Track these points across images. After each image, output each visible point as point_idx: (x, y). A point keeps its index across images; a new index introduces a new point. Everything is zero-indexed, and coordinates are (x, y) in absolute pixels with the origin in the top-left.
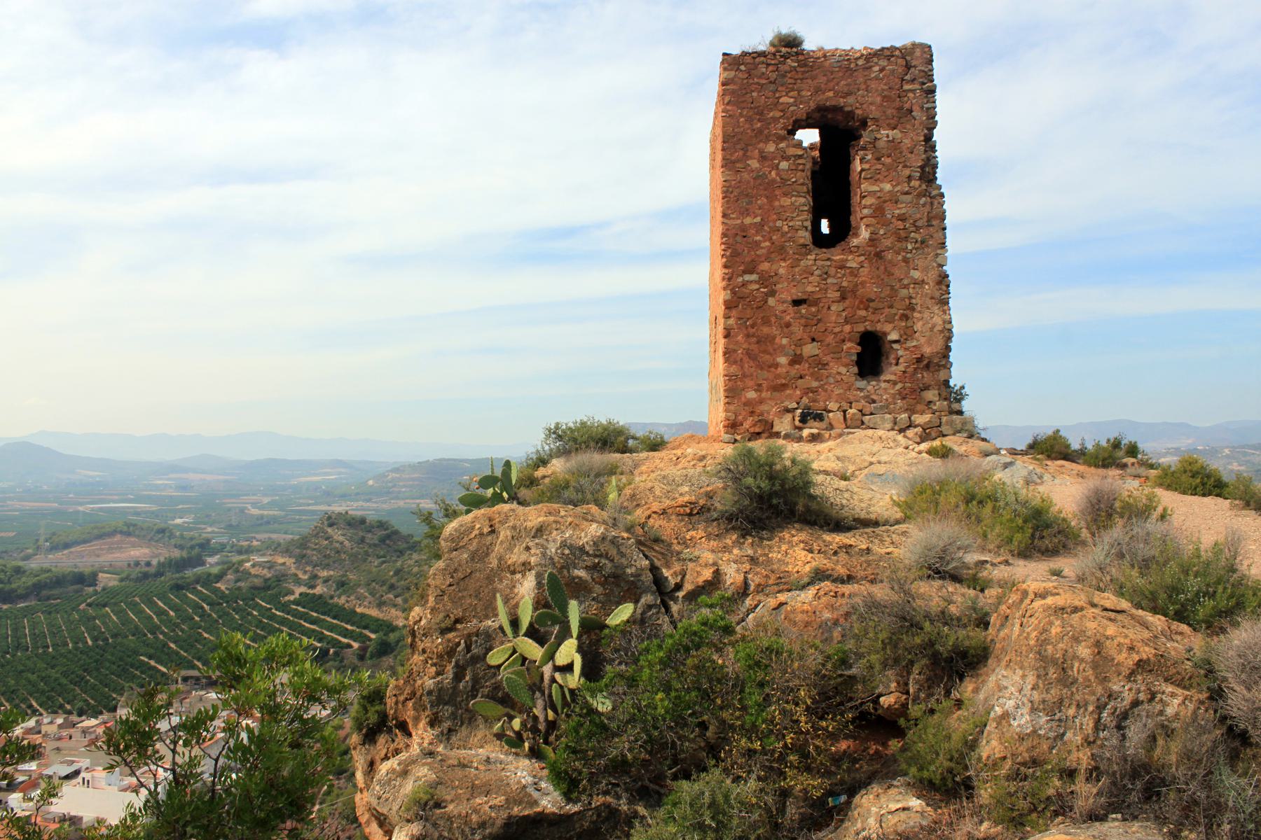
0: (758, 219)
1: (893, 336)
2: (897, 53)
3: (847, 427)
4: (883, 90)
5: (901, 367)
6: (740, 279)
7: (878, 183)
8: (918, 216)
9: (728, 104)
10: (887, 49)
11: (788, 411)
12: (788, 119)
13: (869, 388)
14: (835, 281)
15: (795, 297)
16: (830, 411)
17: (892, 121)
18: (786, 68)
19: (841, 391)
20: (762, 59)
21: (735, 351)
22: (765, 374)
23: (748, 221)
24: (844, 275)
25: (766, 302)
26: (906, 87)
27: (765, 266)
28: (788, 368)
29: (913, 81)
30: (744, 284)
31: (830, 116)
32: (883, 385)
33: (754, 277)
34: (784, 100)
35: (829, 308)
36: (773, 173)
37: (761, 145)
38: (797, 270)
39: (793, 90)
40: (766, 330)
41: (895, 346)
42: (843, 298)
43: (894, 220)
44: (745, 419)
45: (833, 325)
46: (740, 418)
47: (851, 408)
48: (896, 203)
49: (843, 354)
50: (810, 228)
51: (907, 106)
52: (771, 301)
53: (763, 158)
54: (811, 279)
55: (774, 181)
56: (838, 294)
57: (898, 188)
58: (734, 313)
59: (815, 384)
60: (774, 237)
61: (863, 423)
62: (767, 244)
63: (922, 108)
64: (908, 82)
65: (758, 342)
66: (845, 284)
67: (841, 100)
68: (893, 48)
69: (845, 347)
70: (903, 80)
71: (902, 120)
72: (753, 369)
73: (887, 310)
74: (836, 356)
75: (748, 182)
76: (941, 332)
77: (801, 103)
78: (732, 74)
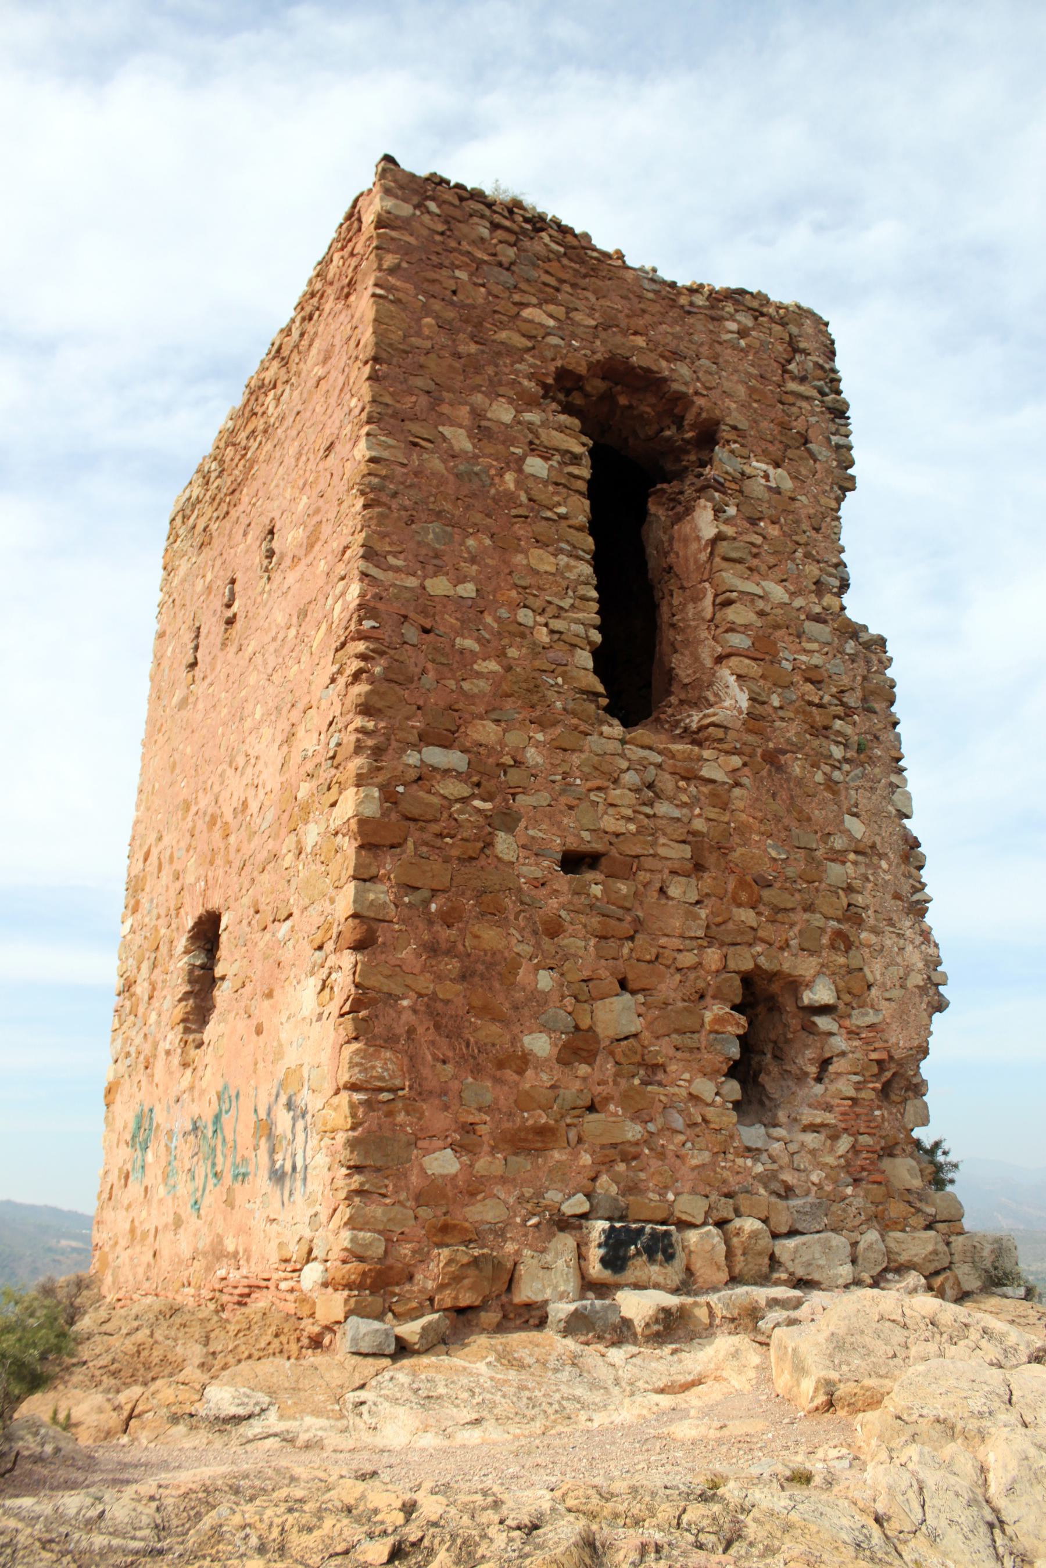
0: (468, 590)
1: (822, 993)
2: (771, 310)
3: (734, 1280)
4: (750, 375)
5: (845, 1087)
6: (412, 758)
7: (756, 577)
8: (845, 681)
9: (392, 271)
10: (751, 294)
11: (564, 1224)
12: (544, 360)
13: (776, 1147)
14: (676, 813)
15: (573, 844)
16: (684, 1225)
17: (771, 448)
19: (705, 1157)
20: (481, 207)
21: (393, 998)
22: (486, 1091)
23: (439, 586)
24: (696, 801)
25: (489, 844)
26: (792, 386)
27: (486, 732)
28: (558, 1071)
29: (803, 380)
30: (423, 777)
31: (623, 401)
32: (810, 1139)
33: (455, 759)
35: (662, 891)
36: (509, 478)
37: (478, 398)
38: (575, 759)
39: (553, 301)
40: (490, 936)
41: (824, 1023)
42: (699, 867)
43: (797, 678)
44: (423, 1257)
45: (677, 943)
46: (406, 1250)
47: (738, 1214)
48: (799, 637)
49: (703, 1038)
51: (798, 426)
54: (615, 794)
55: (511, 498)
56: (687, 851)
57: (799, 602)
58: (388, 865)
59: (633, 1131)
60: (513, 652)
61: (774, 1262)
62: (493, 666)
63: (829, 440)
65: (463, 977)
66: (699, 825)
67: (664, 364)
68: (762, 298)
69: (708, 1016)
70: (785, 371)
71: (790, 453)
72: (449, 1068)
73: (800, 917)
74: (687, 1040)
75: (442, 481)
76: (922, 990)
77: (574, 336)
78: (406, 210)
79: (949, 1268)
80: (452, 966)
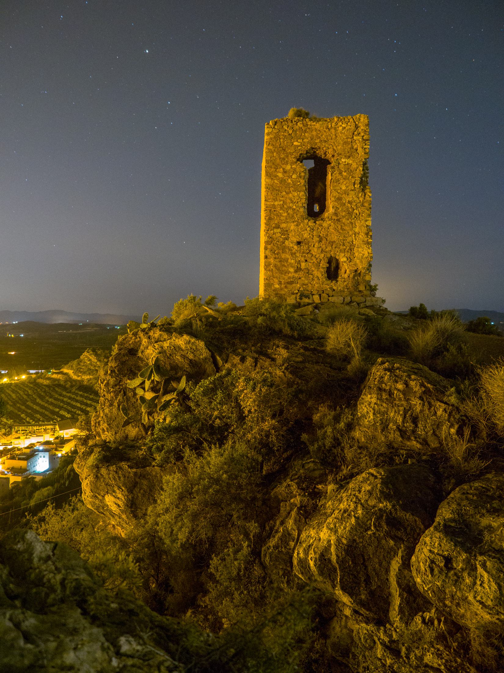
11: (293, 294)
15: (298, 240)
18: (297, 127)
27: (283, 225)
33: (279, 230)
34: (296, 143)
50: (306, 207)
51: (355, 147)
52: (287, 242)
53: (285, 172)
55: (289, 184)
59: (306, 282)
64: (356, 135)
79: (365, 302)
80: (277, 260)
